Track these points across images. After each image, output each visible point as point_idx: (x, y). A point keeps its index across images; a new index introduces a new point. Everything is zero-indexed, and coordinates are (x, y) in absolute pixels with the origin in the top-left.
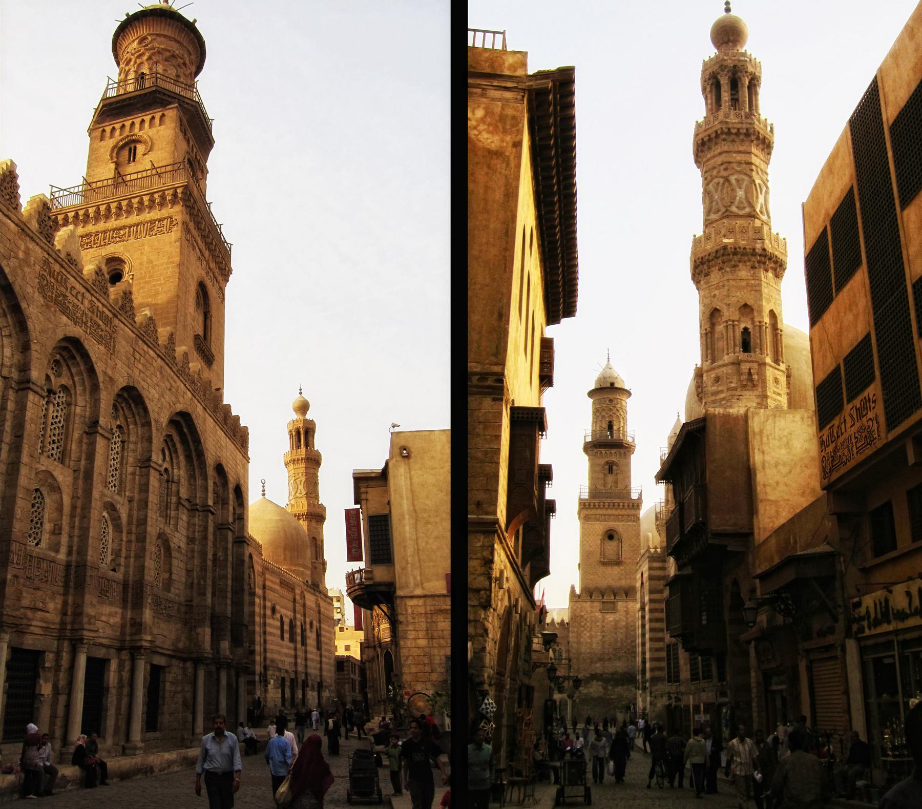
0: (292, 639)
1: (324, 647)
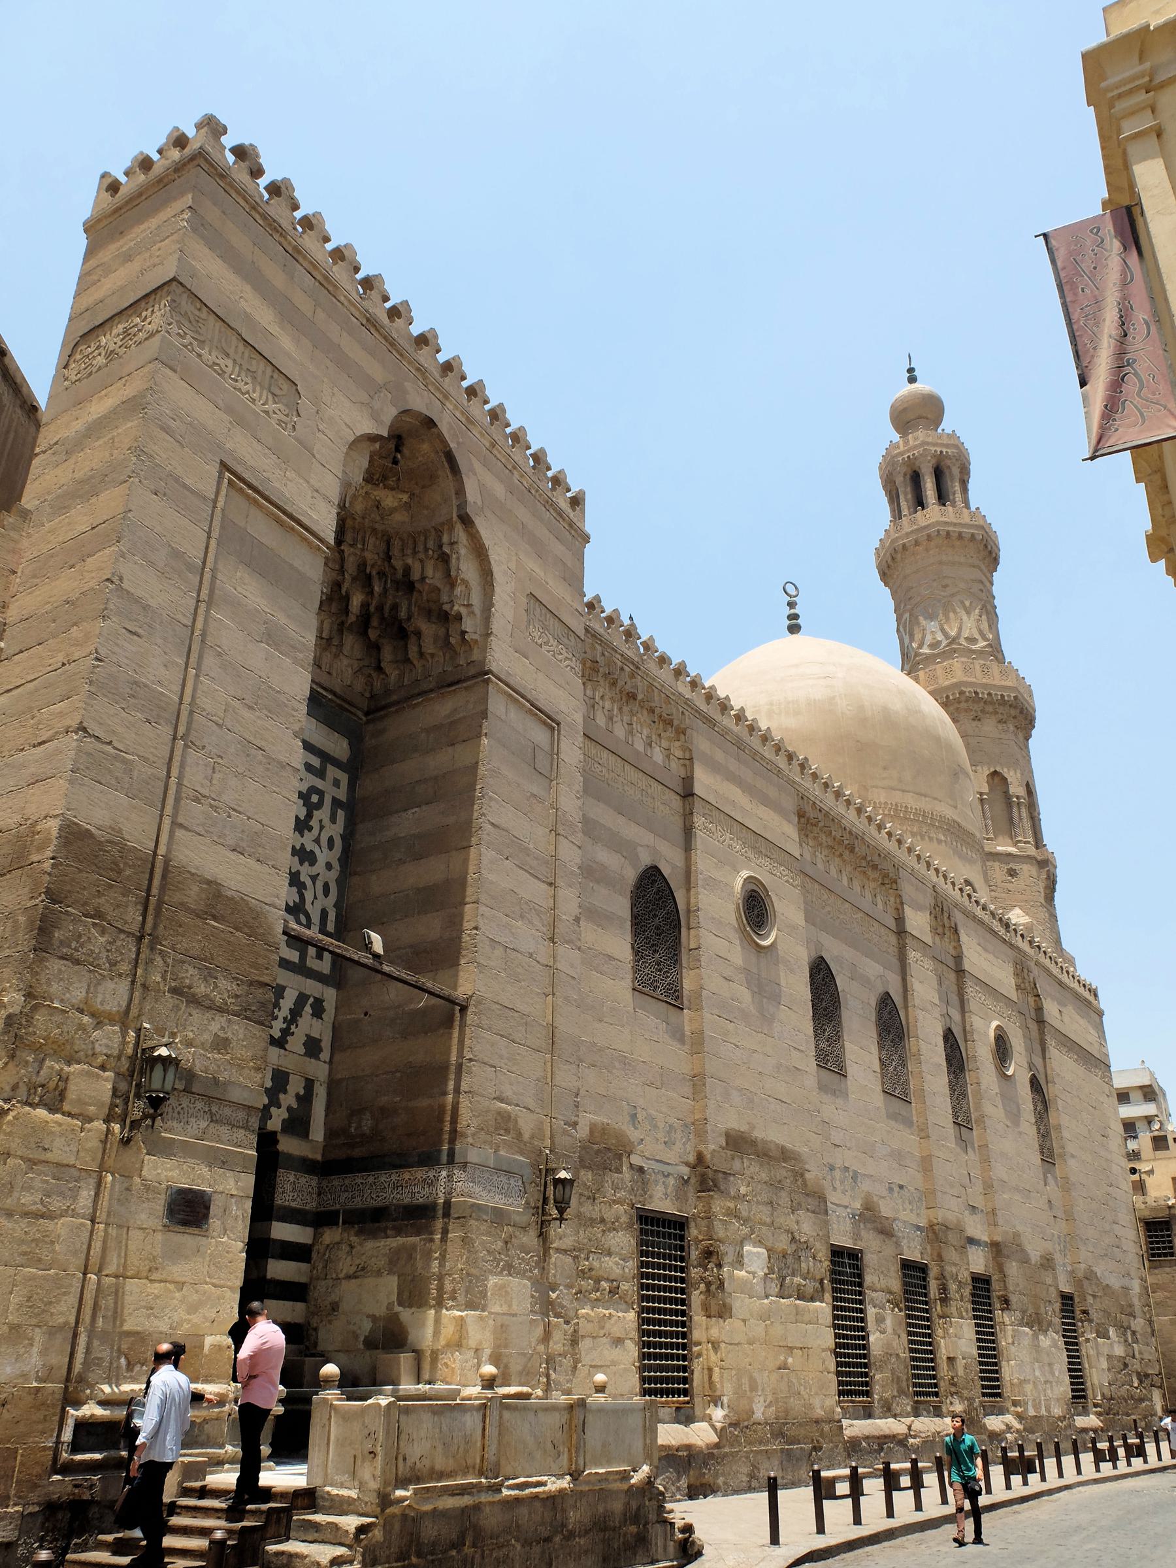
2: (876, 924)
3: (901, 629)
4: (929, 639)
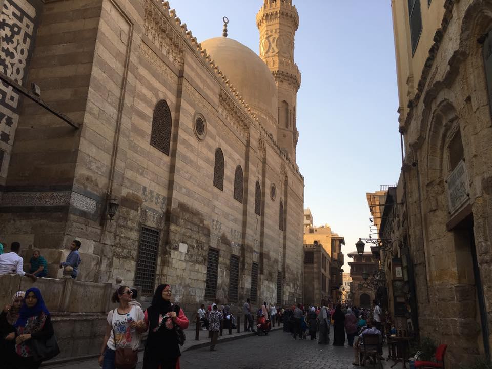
0: (240, 193)
1: (289, 228)
2: (240, 142)
3: (261, 45)
4: (271, 50)
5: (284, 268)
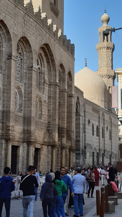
1: (113, 138)
4: (103, 64)
5: (111, 153)
